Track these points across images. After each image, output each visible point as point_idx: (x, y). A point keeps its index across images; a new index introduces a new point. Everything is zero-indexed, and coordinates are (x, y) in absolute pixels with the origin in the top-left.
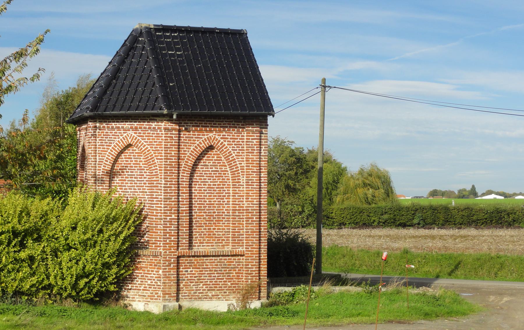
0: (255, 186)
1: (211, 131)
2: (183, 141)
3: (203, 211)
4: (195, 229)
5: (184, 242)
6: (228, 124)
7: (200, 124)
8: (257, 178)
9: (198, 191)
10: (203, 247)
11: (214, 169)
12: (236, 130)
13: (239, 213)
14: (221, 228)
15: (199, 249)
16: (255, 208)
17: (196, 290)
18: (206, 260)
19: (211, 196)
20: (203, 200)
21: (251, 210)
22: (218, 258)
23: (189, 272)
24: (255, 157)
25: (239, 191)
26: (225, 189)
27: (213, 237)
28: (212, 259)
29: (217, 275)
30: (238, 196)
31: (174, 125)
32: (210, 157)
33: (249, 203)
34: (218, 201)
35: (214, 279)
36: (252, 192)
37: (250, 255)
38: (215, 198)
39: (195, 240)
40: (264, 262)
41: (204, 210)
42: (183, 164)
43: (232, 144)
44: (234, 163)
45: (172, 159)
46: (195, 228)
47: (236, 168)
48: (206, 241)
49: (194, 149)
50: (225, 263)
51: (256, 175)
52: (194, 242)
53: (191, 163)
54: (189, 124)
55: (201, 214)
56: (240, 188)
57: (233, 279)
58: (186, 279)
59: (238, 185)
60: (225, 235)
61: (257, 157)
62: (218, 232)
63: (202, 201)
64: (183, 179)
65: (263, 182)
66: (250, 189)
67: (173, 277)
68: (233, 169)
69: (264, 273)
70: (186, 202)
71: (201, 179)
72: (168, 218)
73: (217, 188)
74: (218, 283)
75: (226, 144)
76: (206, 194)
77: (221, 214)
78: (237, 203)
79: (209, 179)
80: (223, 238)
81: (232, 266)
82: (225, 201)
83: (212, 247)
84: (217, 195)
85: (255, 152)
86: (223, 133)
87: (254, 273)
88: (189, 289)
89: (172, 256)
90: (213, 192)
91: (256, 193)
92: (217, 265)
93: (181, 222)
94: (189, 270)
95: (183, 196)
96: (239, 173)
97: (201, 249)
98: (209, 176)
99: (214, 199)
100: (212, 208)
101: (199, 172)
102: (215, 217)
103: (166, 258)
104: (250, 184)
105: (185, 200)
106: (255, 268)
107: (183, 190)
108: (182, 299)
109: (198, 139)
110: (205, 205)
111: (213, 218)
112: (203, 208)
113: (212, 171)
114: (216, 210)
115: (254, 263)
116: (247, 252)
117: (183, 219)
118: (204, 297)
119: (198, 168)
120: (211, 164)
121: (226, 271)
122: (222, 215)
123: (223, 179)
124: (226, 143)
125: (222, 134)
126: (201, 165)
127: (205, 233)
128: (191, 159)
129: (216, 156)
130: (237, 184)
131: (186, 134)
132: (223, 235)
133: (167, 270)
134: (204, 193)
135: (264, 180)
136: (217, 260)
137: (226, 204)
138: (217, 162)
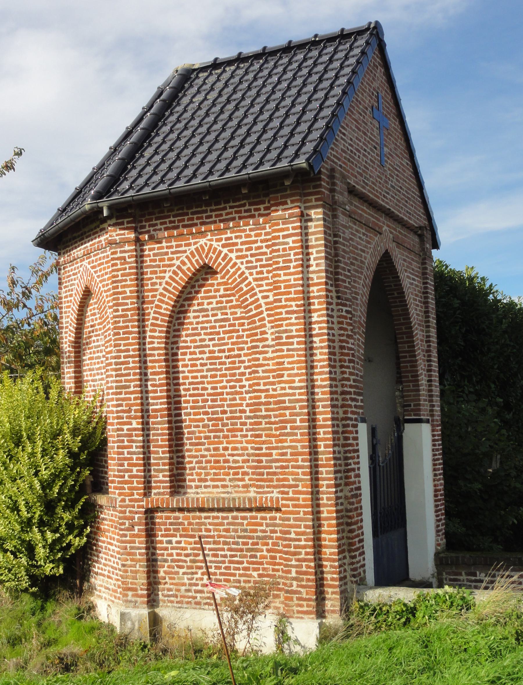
0: (295, 346)
1: (202, 234)
2: (148, 263)
3: (201, 410)
4: (189, 450)
5: (161, 478)
6: (236, 212)
7: (179, 221)
8: (298, 327)
9: (189, 368)
10: (206, 490)
11: (220, 317)
12: (251, 223)
13: (267, 410)
14: (239, 446)
15: (198, 493)
16: (297, 397)
17: (190, 585)
18: (206, 518)
19: (215, 376)
20: (200, 386)
21: (290, 401)
22: (230, 515)
23: (174, 545)
24: (292, 277)
25: (265, 359)
26: (243, 358)
27: (224, 468)
28: (218, 518)
29: (229, 553)
30: (264, 371)
31: (126, 232)
32: (210, 291)
33: (283, 385)
34: (231, 387)
35: (224, 562)
36: (290, 360)
37: (291, 509)
38: (225, 379)
39: (189, 475)
40: (329, 526)
41: (204, 407)
42: (152, 312)
43: (247, 256)
44: (251, 297)
45: (127, 304)
46: (188, 447)
47: (257, 308)
48: (212, 476)
49: (171, 278)
50: (245, 527)
51: (296, 318)
52: (188, 478)
53: (166, 309)
54: (159, 227)
55: (199, 417)
56: (267, 352)
57: (262, 563)
58: (169, 558)
59: (263, 347)
60: (248, 461)
61: (296, 276)
62: (233, 455)
63: (198, 389)
64: (153, 343)
65: (318, 335)
66: (285, 353)
67: (140, 554)
68: (251, 310)
69: (331, 554)
70: (161, 391)
71: (195, 341)
72: (125, 427)
73: (228, 357)
74: (232, 571)
75: (234, 258)
76: (205, 373)
77: (238, 414)
78: (262, 387)
79: (210, 340)
80: (246, 470)
81: (260, 534)
82: (244, 386)
83: (223, 490)
84: (228, 372)
85: (292, 265)
86: (226, 233)
87: (303, 551)
88: (176, 581)
89: (136, 509)
90: (219, 367)
91: (299, 362)
92: (227, 531)
93: (154, 435)
94: (174, 539)
95: (155, 380)
96: (263, 319)
97: (202, 493)
98: (211, 334)
99: (222, 381)
100: (219, 403)
101: (190, 327)
102: (225, 421)
103: (125, 512)
104: (284, 340)
105: (159, 389)
106: (306, 540)
107: (154, 367)
108: (164, 601)
109: (178, 255)
110: (206, 397)
111: (223, 425)
112: (200, 404)
113: (215, 321)
114: (228, 406)
115: (303, 529)
116: (284, 502)
117: (157, 429)
118: (205, 601)
119: (189, 318)
120: (214, 305)
121: (246, 544)
122: (241, 418)
123: (238, 337)
124: (233, 255)
125: (224, 236)
126: (194, 311)
127: (209, 458)
128: (166, 300)
129: (222, 288)
130: (261, 344)
131: (154, 249)
132: (244, 461)
133: (128, 538)
134: (202, 371)
135: (320, 328)
136: (227, 518)
137: (247, 392)
138: (224, 299)
